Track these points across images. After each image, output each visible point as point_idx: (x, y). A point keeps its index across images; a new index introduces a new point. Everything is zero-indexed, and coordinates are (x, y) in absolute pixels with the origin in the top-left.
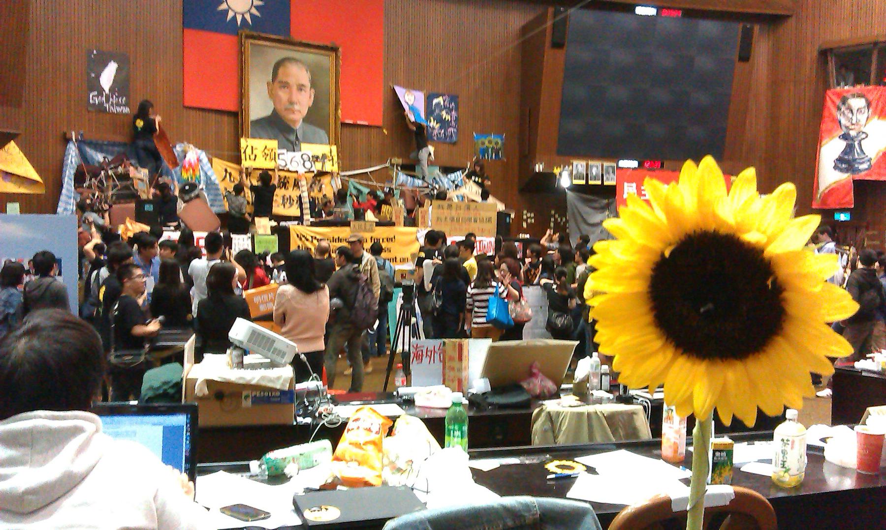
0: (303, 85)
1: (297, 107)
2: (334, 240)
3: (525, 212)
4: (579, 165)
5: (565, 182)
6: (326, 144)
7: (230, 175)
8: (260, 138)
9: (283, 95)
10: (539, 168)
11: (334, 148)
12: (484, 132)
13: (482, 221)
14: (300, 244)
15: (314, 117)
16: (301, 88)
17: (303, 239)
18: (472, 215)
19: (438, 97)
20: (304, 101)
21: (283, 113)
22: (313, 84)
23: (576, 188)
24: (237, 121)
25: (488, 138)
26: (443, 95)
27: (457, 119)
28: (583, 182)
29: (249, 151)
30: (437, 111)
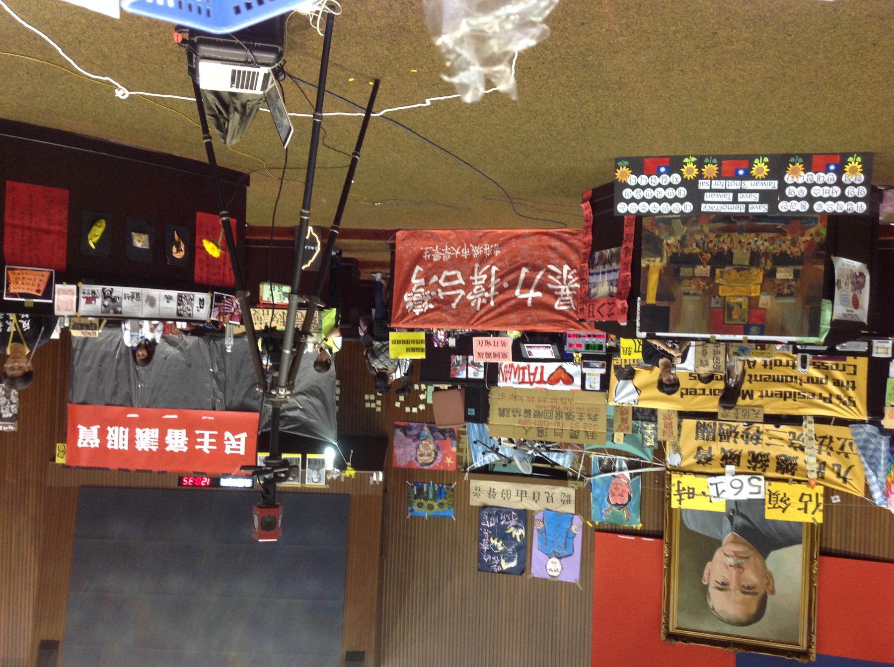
0: (720, 589)
1: (731, 561)
2: (793, 396)
3: (379, 409)
4: (314, 480)
5: (329, 455)
6: (686, 510)
7: (838, 475)
8: (788, 522)
9: (751, 577)
10: (378, 477)
11: (675, 504)
12: (439, 521)
13: (516, 412)
14: (851, 392)
15: (702, 547)
16: (723, 586)
17: (846, 399)
18: (533, 422)
19: (509, 572)
20: (719, 567)
21: (751, 553)
22: (705, 589)
23: (316, 446)
24: (824, 547)
25: (431, 513)
26: (502, 572)
27: (481, 538)
28: (309, 456)
29: (811, 506)
30: (510, 550)
